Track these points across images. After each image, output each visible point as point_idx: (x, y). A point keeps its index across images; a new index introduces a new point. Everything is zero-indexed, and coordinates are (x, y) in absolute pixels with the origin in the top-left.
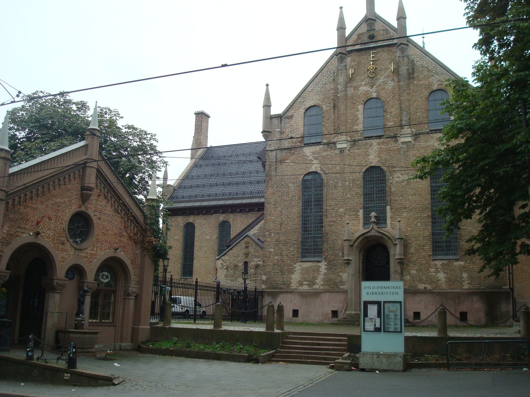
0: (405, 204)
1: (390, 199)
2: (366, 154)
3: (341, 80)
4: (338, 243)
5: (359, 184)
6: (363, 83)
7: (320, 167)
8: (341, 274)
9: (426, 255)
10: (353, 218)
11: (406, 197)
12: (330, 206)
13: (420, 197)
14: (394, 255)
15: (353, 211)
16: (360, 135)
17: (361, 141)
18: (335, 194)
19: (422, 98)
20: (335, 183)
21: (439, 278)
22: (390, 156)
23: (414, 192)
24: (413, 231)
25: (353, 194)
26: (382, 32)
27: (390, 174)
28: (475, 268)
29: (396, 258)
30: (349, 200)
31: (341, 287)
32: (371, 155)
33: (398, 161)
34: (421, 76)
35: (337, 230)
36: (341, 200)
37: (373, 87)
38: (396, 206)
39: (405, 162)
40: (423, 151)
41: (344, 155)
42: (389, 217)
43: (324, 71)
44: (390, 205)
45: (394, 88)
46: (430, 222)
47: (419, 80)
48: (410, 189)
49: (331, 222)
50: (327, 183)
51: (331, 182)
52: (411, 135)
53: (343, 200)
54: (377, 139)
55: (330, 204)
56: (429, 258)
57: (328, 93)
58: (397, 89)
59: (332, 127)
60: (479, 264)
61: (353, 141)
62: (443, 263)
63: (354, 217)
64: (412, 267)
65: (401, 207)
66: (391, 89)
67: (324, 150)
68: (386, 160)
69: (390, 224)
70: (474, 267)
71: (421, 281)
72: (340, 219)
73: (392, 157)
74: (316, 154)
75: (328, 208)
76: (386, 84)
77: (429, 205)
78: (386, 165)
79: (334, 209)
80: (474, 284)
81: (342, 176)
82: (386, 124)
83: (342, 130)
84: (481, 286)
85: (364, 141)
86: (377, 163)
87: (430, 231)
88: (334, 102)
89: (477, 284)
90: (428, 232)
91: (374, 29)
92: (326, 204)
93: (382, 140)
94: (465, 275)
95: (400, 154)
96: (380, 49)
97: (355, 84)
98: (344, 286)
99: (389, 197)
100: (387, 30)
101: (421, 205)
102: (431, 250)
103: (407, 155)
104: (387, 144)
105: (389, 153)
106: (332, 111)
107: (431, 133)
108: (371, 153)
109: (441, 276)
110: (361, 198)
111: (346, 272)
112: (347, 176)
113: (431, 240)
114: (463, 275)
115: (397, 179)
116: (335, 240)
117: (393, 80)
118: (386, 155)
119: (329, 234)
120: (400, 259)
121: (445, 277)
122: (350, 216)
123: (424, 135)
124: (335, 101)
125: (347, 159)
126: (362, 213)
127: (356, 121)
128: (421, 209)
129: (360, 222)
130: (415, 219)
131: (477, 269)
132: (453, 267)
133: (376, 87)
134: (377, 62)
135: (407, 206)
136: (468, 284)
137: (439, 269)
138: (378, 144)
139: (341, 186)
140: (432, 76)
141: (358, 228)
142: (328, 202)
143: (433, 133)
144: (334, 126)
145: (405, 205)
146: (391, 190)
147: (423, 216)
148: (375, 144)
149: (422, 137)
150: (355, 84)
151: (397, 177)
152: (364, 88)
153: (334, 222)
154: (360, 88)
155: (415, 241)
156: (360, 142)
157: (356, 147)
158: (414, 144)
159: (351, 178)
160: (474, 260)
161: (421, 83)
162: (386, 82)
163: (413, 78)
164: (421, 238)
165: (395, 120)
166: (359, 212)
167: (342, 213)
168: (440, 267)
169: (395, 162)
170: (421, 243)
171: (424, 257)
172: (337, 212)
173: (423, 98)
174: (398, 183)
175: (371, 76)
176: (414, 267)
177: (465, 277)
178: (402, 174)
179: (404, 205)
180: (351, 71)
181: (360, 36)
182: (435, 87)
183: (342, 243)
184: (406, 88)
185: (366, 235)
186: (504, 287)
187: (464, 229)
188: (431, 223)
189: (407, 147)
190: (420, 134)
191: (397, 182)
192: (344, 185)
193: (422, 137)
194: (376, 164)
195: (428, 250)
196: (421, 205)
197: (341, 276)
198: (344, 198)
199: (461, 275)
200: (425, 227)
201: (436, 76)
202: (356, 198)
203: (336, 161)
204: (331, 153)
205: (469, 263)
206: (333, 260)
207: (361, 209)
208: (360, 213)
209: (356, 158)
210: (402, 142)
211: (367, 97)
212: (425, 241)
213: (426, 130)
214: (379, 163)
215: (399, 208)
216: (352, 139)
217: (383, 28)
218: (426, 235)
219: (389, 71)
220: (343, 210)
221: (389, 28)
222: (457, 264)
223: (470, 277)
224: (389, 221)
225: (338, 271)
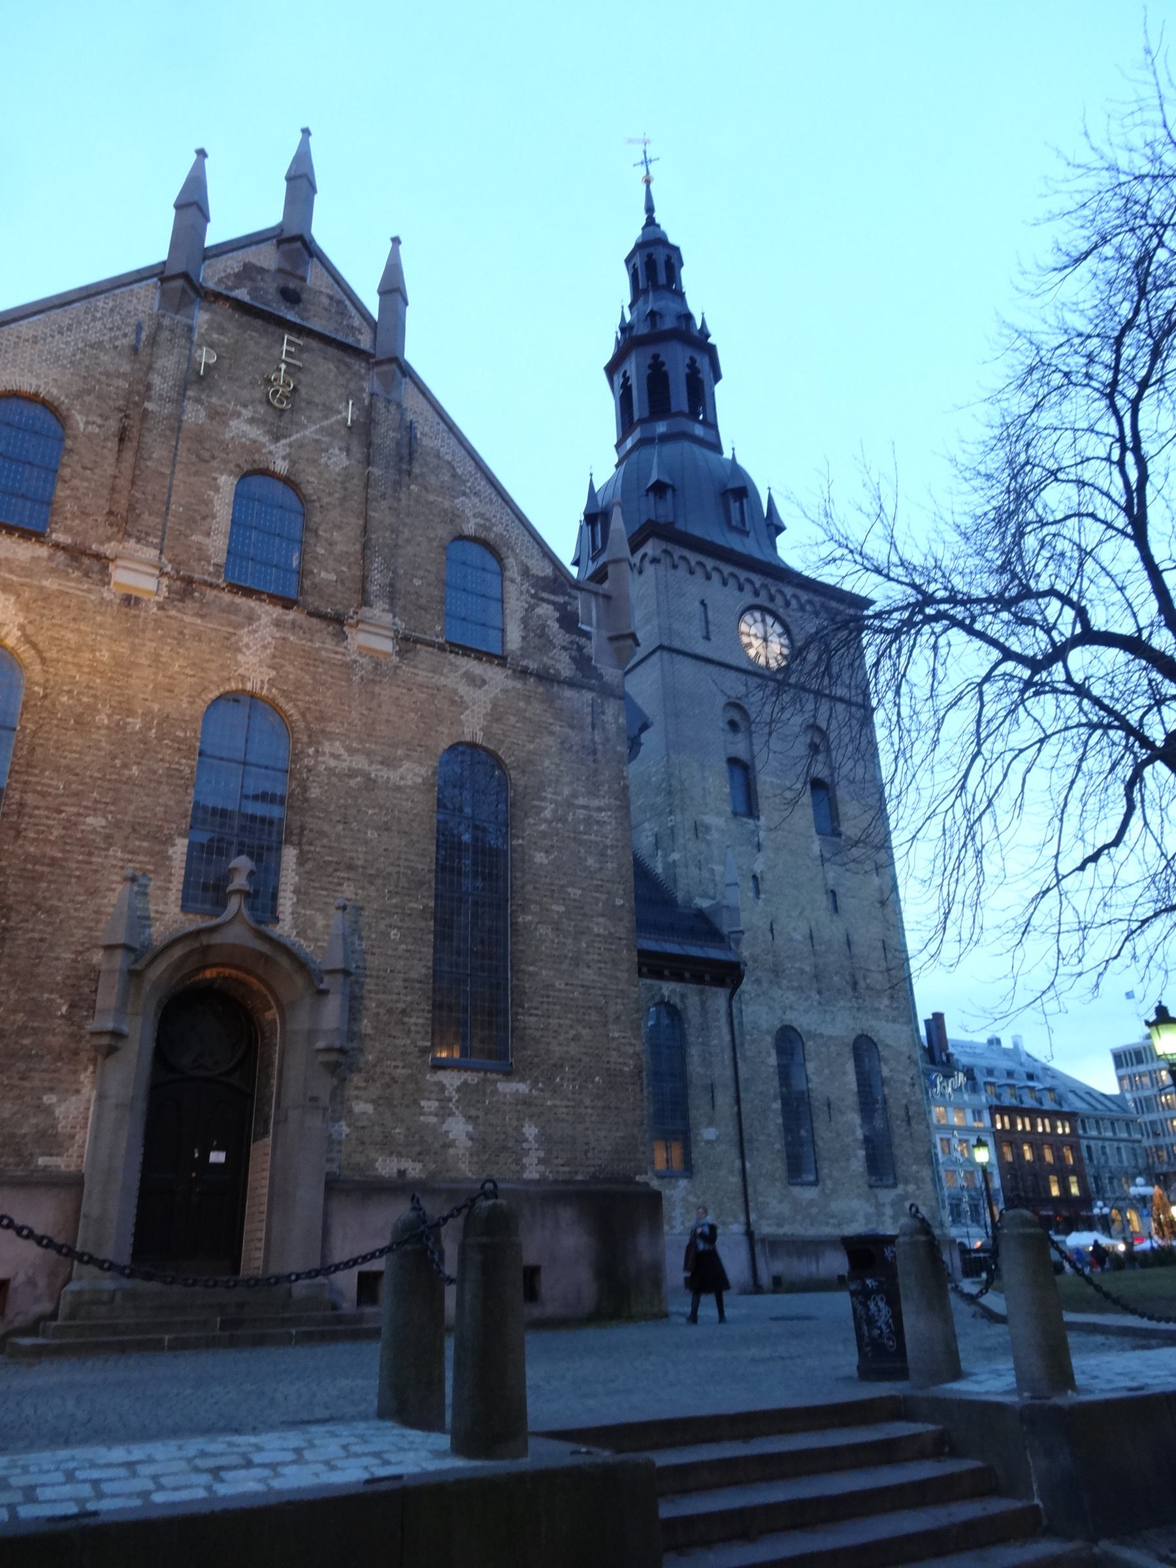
0: (352, 854)
1: (299, 824)
2: (228, 643)
3: (168, 364)
4: (57, 959)
5: (186, 738)
6: (247, 413)
7: (22, 627)
8: (49, 1099)
9: (411, 1049)
10: (140, 862)
11: (359, 831)
12: (44, 795)
13: (403, 842)
14: (312, 1034)
15: (145, 838)
16: (211, 569)
17: (215, 592)
18: (75, 752)
19: (430, 540)
20: (80, 710)
21: (451, 1136)
22: (314, 678)
23: (385, 819)
24: (373, 954)
25: (155, 773)
26: (325, 301)
27: (310, 736)
28: (561, 1106)
29: (321, 1044)
30: (136, 789)
31: (41, 1161)
32: (248, 653)
33: (342, 704)
34: (433, 480)
35: (60, 899)
36: (99, 782)
37: (276, 439)
38: (319, 853)
39: (365, 712)
40: (424, 696)
41: (135, 616)
42: (292, 888)
43: (102, 303)
44: (300, 844)
45: (347, 475)
46: (430, 933)
47: (426, 488)
48: (374, 807)
49: (36, 860)
50: (45, 696)
51: (64, 699)
53: (106, 784)
54: (275, 605)
55: (43, 785)
56: (419, 1061)
57: (103, 378)
59: (102, 502)
60: (570, 1096)
61: (182, 579)
62: (465, 1083)
63: (148, 863)
64: (357, 1088)
65: (335, 859)
66: (339, 475)
67: (53, 571)
68: (299, 685)
69: (292, 913)
70: (558, 1102)
71: (387, 1145)
72: (81, 857)
73: (322, 684)
74: (11, 571)
75: (30, 799)
76: (323, 450)
77: (432, 875)
78: (300, 703)
79: (61, 812)
80: (556, 1165)
81: (118, 691)
82: (312, 572)
83: (148, 526)
84: (576, 1173)
85: (227, 597)
86: (266, 686)
87: (430, 964)
88: (127, 422)
89: (563, 1165)
90: (421, 969)
91: (303, 279)
92: (26, 783)
93: (291, 615)
94: (530, 1131)
95: (349, 680)
96: (314, 344)
97: (214, 400)
98: (58, 1155)
99: (297, 817)
101: (408, 867)
102: (427, 1033)
103: (373, 695)
104: (308, 636)
105: (312, 668)
106: (109, 444)
107: (451, 652)
108: (247, 646)
109: (458, 1128)
110: (187, 794)
111: (78, 1091)
112: (141, 696)
113: (430, 995)
114: (524, 1130)
115: (332, 763)
116: (42, 940)
117: (348, 450)
118: (302, 669)
119: (19, 912)
120: (342, 1051)
121: (467, 1133)
122: (132, 852)
123: (430, 649)
124: (127, 416)
125: (149, 634)
126: (185, 850)
127: (204, 518)
128: (403, 882)
129: (171, 886)
130: (382, 911)
131: (565, 1110)
132: (495, 1099)
133: (290, 446)
134: (300, 376)
135: (360, 863)
136: (541, 1161)
137: (451, 1105)
138: (278, 624)
139: (108, 728)
140: (464, 494)
141: (161, 908)
142: (36, 775)
143: (457, 654)
144: (111, 500)
145: (352, 858)
146: (307, 795)
147: (410, 909)
148: (265, 620)
149: (423, 651)
150: (214, 400)
151: (334, 756)
152: (246, 427)
153: (53, 862)
154: (231, 423)
155: (377, 993)
156: (211, 594)
157: (189, 604)
159: (156, 707)
160: (558, 1080)
161: (431, 498)
162: (323, 446)
163: (409, 473)
164: (399, 983)
165: (342, 571)
166: (173, 845)
167: (94, 831)
168: (456, 1097)
169: (330, 701)
170: (397, 1001)
171: (403, 1053)
172: (70, 825)
173: (435, 544)
174: (335, 774)
175: (275, 403)
176: (365, 1088)
177: (530, 1139)
178: (351, 751)
179: (349, 854)
180: (205, 357)
181: (249, 272)
182: (470, 528)
183: (75, 961)
184: (389, 491)
185: (205, 940)
186: (638, 1178)
187: (531, 974)
188: (431, 937)
189: (375, 668)
190: (417, 641)
191: (331, 771)
192: (120, 727)
193: (422, 654)
194: (262, 688)
195: (419, 1029)
196: (408, 867)
197: (48, 1110)
198: (114, 777)
199: (519, 1129)
200: (411, 947)
201: (476, 500)
202: (164, 788)
203: (101, 626)
204: (82, 590)
205: (542, 1090)
206: (22, 1031)
207: (180, 835)
208: (175, 848)
209: (188, 644)
211: (254, 461)
212: (409, 998)
213: (437, 637)
214: (274, 690)
215: (331, 862)
216: (178, 572)
218: (414, 975)
219: (338, 422)
220: (104, 823)
221: (347, 302)
222: (507, 1090)
223: (545, 1139)
224: (286, 903)
225: (37, 1083)
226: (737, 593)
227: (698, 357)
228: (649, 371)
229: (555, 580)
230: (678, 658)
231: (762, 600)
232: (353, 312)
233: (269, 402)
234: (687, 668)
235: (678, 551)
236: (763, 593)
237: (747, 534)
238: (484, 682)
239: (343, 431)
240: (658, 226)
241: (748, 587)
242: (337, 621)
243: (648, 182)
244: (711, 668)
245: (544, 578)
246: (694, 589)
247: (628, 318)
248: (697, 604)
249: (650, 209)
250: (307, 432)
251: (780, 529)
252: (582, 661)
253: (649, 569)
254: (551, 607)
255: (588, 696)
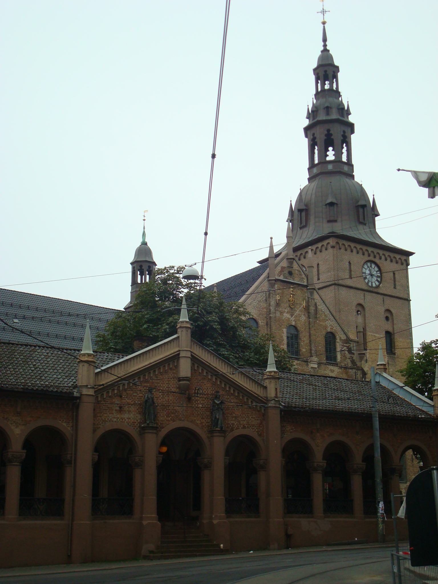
3: (273, 303)
26: (297, 272)
37: (292, 316)
52: (316, 363)
58: (307, 323)
93: (299, 362)
100: (300, 271)
107: (328, 365)
117: (305, 315)
127: (282, 341)
140: (327, 320)
152: (286, 315)
158: (318, 371)
161: (321, 323)
201: (330, 321)
210: (311, 367)
217: (298, 269)
219: (302, 307)
221: (301, 271)
226: (362, 256)
227: (346, 130)
228: (325, 138)
229: (346, 340)
230: (340, 288)
231: (371, 258)
232: (302, 273)
233: (290, 306)
234: (344, 292)
235: (341, 242)
236: (372, 255)
237: (365, 224)
238: (334, 371)
239: (304, 310)
240: (329, 51)
241: (366, 253)
242: (306, 362)
243: (324, 23)
244: (352, 291)
245: (344, 340)
246: (347, 256)
247: (315, 101)
248: (347, 263)
249: (325, 40)
250: (297, 313)
251: (378, 215)
252: (353, 362)
253: (330, 250)
254: (346, 348)
255: (354, 370)
